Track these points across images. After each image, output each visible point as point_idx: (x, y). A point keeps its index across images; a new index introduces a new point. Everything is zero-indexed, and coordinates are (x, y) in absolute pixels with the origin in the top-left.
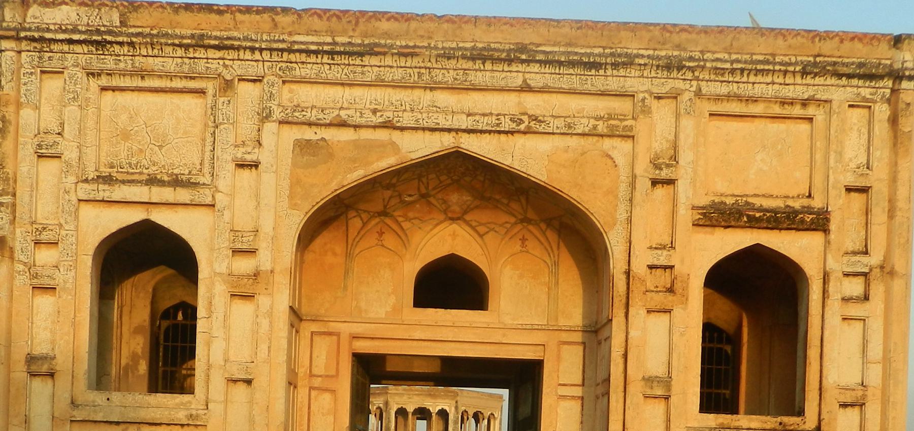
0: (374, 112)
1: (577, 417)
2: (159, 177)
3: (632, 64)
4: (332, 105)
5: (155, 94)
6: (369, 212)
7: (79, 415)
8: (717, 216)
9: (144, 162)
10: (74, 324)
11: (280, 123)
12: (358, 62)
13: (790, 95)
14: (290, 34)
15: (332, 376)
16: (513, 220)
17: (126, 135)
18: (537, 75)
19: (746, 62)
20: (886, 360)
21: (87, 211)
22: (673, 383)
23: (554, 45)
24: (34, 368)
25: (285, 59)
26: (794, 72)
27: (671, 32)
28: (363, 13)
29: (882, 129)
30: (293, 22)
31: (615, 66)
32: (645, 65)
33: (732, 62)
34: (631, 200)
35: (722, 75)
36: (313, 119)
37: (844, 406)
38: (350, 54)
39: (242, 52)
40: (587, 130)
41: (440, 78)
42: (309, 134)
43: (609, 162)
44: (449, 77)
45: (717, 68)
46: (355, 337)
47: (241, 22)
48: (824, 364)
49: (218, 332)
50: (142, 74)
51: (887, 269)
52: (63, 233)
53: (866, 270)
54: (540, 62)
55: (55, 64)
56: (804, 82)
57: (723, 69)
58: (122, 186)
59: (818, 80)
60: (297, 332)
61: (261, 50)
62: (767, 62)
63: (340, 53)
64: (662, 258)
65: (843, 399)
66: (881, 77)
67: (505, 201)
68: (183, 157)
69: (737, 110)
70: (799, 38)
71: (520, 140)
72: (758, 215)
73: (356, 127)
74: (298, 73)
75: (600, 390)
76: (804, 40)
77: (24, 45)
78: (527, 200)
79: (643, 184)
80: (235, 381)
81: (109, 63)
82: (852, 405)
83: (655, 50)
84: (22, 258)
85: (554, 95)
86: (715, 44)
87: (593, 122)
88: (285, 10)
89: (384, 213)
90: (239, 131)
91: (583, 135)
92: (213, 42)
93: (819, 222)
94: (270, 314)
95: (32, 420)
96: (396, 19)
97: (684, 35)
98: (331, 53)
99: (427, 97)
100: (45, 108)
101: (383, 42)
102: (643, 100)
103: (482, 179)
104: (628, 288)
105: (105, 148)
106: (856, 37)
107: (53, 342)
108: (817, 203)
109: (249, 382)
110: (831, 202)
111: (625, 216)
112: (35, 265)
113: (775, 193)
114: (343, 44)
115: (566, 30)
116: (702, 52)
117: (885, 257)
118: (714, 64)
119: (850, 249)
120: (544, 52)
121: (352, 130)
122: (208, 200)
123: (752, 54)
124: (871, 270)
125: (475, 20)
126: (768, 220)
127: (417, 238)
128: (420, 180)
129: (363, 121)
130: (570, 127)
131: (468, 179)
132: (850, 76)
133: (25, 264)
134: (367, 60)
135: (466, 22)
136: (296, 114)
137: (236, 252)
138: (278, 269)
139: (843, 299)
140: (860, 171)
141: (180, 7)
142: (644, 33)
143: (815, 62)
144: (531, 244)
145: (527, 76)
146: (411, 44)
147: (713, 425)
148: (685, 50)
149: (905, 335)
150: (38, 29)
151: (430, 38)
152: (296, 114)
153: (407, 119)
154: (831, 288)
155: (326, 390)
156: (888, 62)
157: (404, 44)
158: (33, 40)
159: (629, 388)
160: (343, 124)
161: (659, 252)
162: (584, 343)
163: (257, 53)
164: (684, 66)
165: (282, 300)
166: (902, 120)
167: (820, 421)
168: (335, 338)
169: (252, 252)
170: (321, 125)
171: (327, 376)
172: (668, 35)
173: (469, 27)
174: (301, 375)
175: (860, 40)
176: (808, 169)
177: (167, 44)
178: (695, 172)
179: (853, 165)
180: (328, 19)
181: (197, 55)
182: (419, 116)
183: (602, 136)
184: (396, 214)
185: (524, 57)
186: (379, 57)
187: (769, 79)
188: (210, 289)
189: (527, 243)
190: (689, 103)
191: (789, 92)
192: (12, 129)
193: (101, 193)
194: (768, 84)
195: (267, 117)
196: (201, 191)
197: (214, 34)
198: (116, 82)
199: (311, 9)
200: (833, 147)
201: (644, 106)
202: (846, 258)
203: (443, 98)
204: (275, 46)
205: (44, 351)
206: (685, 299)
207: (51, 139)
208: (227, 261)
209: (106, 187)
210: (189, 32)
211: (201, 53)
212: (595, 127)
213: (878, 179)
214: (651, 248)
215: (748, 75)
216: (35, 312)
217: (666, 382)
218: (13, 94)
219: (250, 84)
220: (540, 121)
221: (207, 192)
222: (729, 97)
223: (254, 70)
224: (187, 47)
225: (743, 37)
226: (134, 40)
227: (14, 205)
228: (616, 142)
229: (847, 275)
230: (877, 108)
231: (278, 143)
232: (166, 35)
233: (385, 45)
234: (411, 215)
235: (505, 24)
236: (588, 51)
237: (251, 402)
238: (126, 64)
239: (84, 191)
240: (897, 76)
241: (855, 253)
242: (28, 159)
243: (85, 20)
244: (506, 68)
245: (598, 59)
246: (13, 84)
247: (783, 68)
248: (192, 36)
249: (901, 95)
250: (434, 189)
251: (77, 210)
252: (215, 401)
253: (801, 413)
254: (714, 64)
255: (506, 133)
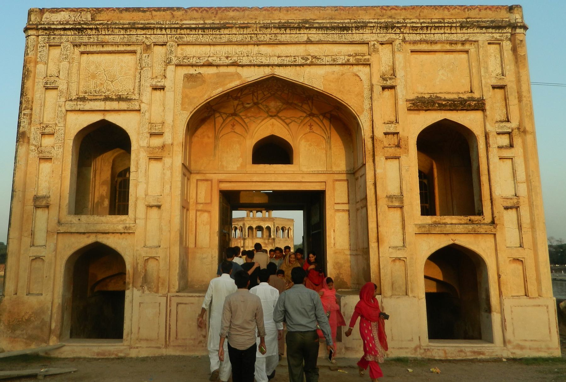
0: (227, 57)
1: (347, 221)
2: (110, 97)
3: (366, 26)
4: (204, 55)
5: (109, 55)
6: (226, 114)
7: (62, 229)
8: (420, 104)
9: (103, 90)
10: (61, 178)
11: (177, 65)
12: (218, 32)
13: (455, 39)
14: (181, 20)
15: (208, 203)
16: (305, 115)
17: (94, 76)
18: (315, 35)
19: (428, 23)
20: (528, 181)
21: (71, 117)
22: (404, 198)
23: (323, 19)
24: (38, 203)
25: (178, 33)
26: (456, 27)
27: (386, 10)
28: (220, 8)
29: (508, 54)
30: (183, 14)
31: (357, 28)
32: (374, 27)
33: (421, 23)
34: (371, 98)
35: (416, 30)
36: (194, 63)
37: (507, 208)
38: (213, 28)
39: (155, 31)
40: (344, 62)
41: (262, 39)
42: (192, 71)
43: (358, 78)
44: (267, 38)
45: (413, 27)
46: (221, 181)
47: (155, 16)
48: (492, 184)
49: (142, 179)
50: (103, 44)
51: (522, 130)
52: (57, 128)
53: (510, 131)
54: (316, 28)
55: (57, 41)
56: (462, 32)
57: (417, 27)
58: (90, 102)
59: (469, 31)
60: (188, 179)
61: (166, 29)
62: (440, 22)
63: (208, 28)
64: (391, 128)
65: (506, 204)
66: (504, 27)
67: (300, 104)
68: (124, 86)
69: (426, 48)
70: (456, 10)
71: (307, 69)
72: (444, 103)
73: (218, 66)
74: (185, 39)
75: (359, 206)
76: (459, 11)
77: (40, 32)
78: (312, 103)
79: (377, 89)
80: (151, 207)
81: (85, 39)
82: (511, 208)
83: (378, 19)
84: (34, 142)
85: (325, 45)
86: (411, 15)
87: (347, 57)
88: (179, 9)
89: (234, 114)
90: (154, 71)
91: (342, 65)
92: (140, 26)
93: (479, 106)
94: (171, 168)
95: (36, 233)
96: (238, 10)
97: (393, 11)
98: (203, 29)
99: (256, 49)
100: (51, 64)
101: (231, 22)
102: (374, 45)
103: (287, 92)
104: (373, 146)
105: (82, 83)
106: (487, 8)
107: (49, 188)
108: (477, 95)
109: (159, 207)
110: (485, 94)
111: (368, 106)
112: (41, 146)
113: (452, 91)
114: (209, 24)
115: (329, 11)
116: (404, 19)
117: (519, 123)
118: (411, 25)
119: (499, 120)
120: (318, 23)
121: (215, 67)
122: (137, 107)
123: (432, 19)
124: (512, 130)
125: (280, 9)
126: (450, 105)
127: (253, 127)
128: (253, 95)
129: (221, 63)
130: (334, 61)
131: (279, 93)
132: (487, 28)
133: (35, 146)
134: (222, 31)
135: (275, 10)
136: (185, 60)
137: (152, 135)
138: (175, 143)
139: (498, 147)
140: (499, 77)
141: (123, 10)
142: (371, 11)
143: (467, 21)
144: (315, 128)
145: (309, 35)
146: (246, 22)
147: (430, 222)
148: (394, 18)
149: (537, 166)
150: (48, 24)
151: (256, 19)
152: (185, 60)
153: (245, 61)
154: (491, 141)
155: (205, 211)
156: (507, 20)
157: (242, 22)
158: (45, 29)
159: (379, 203)
160: (210, 65)
161: (390, 125)
162: (347, 180)
163: (164, 30)
164: (395, 26)
165: (177, 159)
166: (519, 50)
167: (493, 218)
168: (210, 182)
169: (161, 134)
170: (199, 66)
171: (205, 203)
172: (384, 11)
173: (277, 12)
174: (191, 203)
175: (490, 9)
176: (469, 78)
177: (115, 28)
178: (406, 81)
179: (494, 75)
180: (201, 12)
181: (131, 33)
182: (252, 59)
183: (352, 65)
184: (241, 114)
185: (307, 26)
186: (229, 29)
187: (442, 31)
188: (137, 156)
189: (313, 127)
190: (399, 46)
191: (454, 37)
192: (32, 75)
193: (79, 107)
194: (442, 34)
195: (169, 63)
196: (133, 103)
197: (141, 22)
198: (89, 49)
199: (192, 8)
200: (482, 65)
201: (375, 48)
202: (497, 125)
203: (264, 49)
204: (173, 26)
205: (44, 194)
206: (407, 150)
207: (52, 79)
208: (147, 140)
209: (81, 103)
210: (128, 22)
211: (134, 32)
212: (348, 60)
213: (510, 80)
214: (385, 123)
215: (431, 30)
216: (40, 172)
217: (400, 197)
218: (33, 57)
219: (160, 47)
220: (318, 59)
221: (136, 103)
222: (421, 42)
223: (162, 39)
224: (126, 29)
225: (425, 11)
226: (98, 26)
227: (31, 114)
228: (360, 68)
229: (499, 134)
230: (504, 43)
231: (175, 77)
232: (116, 24)
233: (232, 23)
234: (249, 115)
235: (296, 10)
236: (342, 21)
237: (160, 218)
238: (94, 39)
239: (70, 105)
240: (514, 26)
241: (501, 122)
242: (39, 90)
243: (73, 18)
244: (298, 32)
245: (347, 25)
246: (33, 52)
247: (450, 25)
248: (129, 24)
249: (517, 36)
250: (261, 100)
251: (65, 116)
252: (139, 219)
253: (481, 213)
254: (411, 25)
255: (300, 65)
